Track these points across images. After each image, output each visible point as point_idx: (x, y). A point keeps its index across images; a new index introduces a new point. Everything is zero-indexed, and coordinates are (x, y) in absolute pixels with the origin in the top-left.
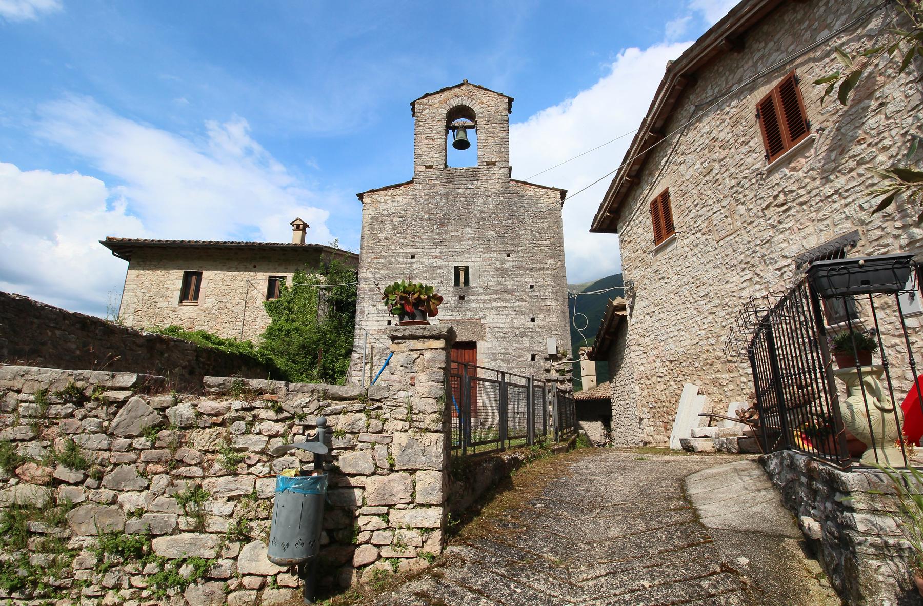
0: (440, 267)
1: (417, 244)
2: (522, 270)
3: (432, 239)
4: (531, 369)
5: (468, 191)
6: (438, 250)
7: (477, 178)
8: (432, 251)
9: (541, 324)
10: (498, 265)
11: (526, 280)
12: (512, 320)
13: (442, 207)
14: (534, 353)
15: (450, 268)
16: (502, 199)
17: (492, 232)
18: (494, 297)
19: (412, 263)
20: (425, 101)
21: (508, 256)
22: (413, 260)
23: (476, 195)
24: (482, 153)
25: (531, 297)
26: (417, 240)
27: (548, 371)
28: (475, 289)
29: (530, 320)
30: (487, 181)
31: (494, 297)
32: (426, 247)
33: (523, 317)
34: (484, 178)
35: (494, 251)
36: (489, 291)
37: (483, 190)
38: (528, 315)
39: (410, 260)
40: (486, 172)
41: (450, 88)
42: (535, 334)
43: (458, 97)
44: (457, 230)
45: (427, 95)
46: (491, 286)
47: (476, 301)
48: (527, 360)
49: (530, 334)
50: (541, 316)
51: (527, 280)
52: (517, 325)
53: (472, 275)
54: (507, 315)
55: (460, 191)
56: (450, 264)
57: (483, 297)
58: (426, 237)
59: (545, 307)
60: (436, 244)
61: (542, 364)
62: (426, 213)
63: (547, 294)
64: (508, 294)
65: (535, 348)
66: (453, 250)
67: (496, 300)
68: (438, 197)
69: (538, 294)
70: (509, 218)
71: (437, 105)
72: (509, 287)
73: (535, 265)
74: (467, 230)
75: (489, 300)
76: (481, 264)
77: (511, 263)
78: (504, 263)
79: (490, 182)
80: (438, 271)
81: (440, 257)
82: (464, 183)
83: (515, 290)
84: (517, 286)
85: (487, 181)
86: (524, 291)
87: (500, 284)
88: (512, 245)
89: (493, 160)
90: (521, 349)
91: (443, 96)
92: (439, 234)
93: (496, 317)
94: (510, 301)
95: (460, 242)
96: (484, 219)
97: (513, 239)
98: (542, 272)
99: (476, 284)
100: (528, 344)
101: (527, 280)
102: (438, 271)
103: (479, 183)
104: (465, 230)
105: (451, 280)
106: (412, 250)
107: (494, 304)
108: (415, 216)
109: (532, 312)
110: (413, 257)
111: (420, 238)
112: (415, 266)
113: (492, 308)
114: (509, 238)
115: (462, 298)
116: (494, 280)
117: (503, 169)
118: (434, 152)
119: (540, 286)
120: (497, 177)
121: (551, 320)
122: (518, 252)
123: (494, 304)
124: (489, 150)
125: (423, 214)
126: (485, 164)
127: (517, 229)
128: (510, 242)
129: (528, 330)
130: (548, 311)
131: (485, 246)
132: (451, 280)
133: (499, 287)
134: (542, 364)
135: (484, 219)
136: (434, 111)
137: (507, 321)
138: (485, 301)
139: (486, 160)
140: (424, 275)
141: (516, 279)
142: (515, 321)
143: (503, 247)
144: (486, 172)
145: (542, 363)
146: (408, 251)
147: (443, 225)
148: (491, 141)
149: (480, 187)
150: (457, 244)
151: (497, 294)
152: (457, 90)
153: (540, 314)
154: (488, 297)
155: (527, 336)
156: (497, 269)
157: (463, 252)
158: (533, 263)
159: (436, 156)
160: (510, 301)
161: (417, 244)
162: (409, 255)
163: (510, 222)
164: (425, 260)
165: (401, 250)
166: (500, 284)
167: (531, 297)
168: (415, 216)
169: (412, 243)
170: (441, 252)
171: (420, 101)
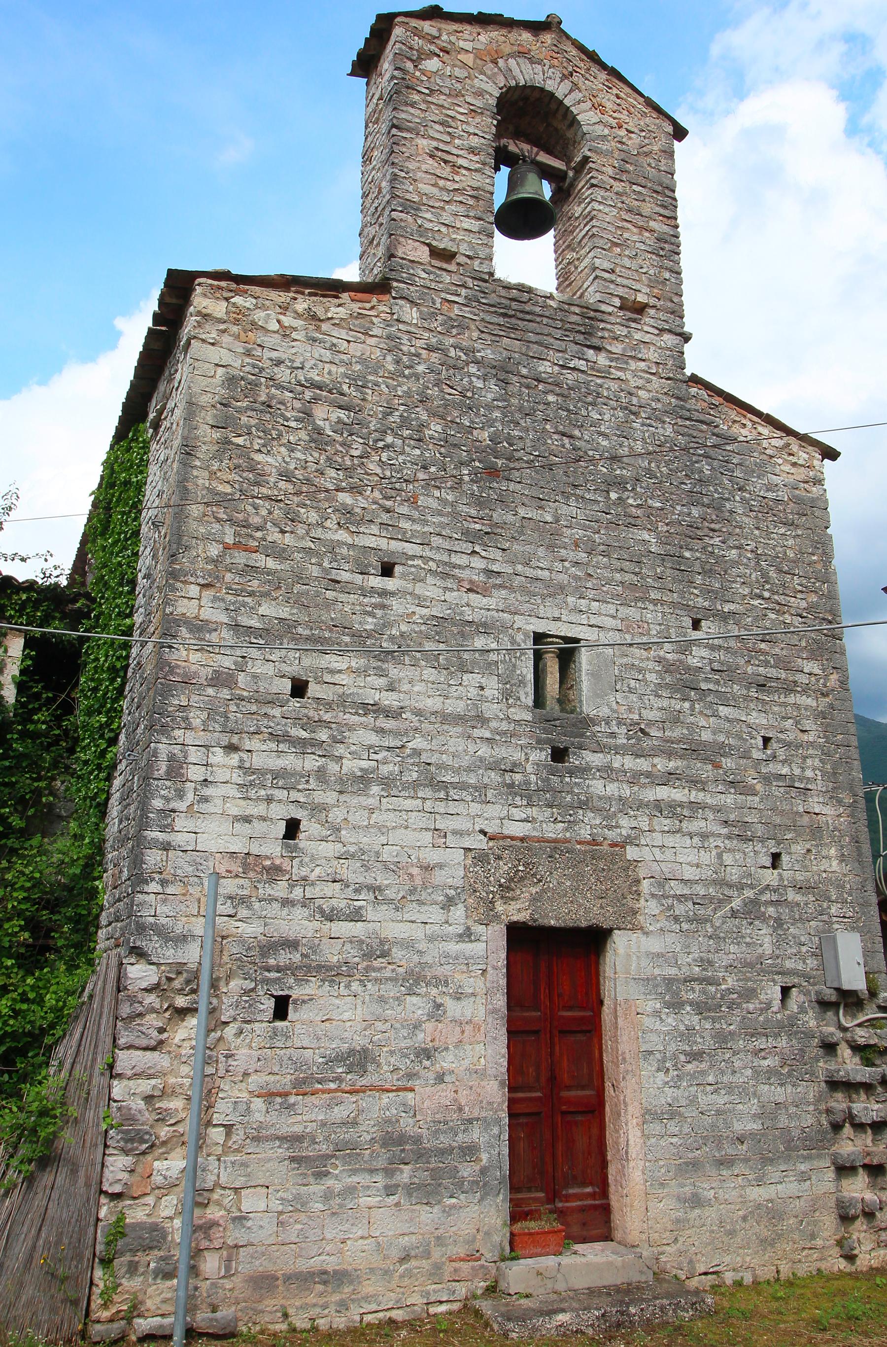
0: (484, 628)
1: (405, 525)
2: (739, 682)
3: (455, 515)
4: (783, 1043)
5: (570, 377)
6: (478, 563)
7: (595, 342)
8: (456, 559)
9: (799, 877)
10: (668, 652)
11: (751, 719)
12: (720, 856)
13: (489, 407)
14: (789, 981)
15: (519, 637)
16: (669, 431)
17: (646, 536)
18: (661, 764)
19: (384, 593)
20: (427, 26)
21: (696, 625)
22: (390, 584)
23: (595, 398)
24: (607, 265)
25: (767, 779)
26: (404, 509)
27: (829, 1048)
28: (603, 728)
29: (768, 862)
30: (624, 358)
31: (661, 764)
32: (436, 541)
33: (749, 848)
34: (617, 348)
35: (655, 602)
36: (647, 743)
37: (614, 386)
38: (762, 840)
39: (376, 582)
40: (621, 331)
41: (510, 24)
42: (785, 911)
43: (532, 61)
44: (540, 502)
45: (434, 13)
46: (651, 723)
47: (608, 773)
48: (769, 1005)
49: (771, 911)
50: (799, 849)
51: (756, 718)
52: (734, 874)
53: (595, 675)
54: (704, 836)
55: (545, 367)
56: (519, 621)
57: (629, 762)
58: (434, 504)
59: (806, 819)
60: (470, 537)
61: (812, 1023)
62: (433, 414)
63: (809, 773)
64: (706, 760)
65: (789, 964)
66: (530, 572)
67: (670, 778)
68: (473, 369)
69: (785, 771)
70: (693, 497)
71: (469, 59)
72: (706, 736)
73: (773, 672)
74: (570, 509)
75: (648, 775)
76: (616, 637)
77: (705, 653)
78: (685, 647)
79: (633, 365)
80: (479, 642)
81: (484, 591)
82: (557, 344)
83: (722, 750)
84: (728, 734)
85: (624, 358)
86: (746, 756)
87: (676, 719)
88: (707, 592)
89: (641, 298)
90: (751, 965)
91: (486, 37)
92: (480, 503)
93: (670, 840)
94: (711, 787)
95: (551, 547)
96: (620, 484)
97: (707, 572)
98: (791, 699)
99: (605, 712)
100: (768, 949)
101: (756, 718)
102: (479, 642)
103: (602, 360)
104: (564, 510)
105: (522, 683)
106: (383, 544)
107: (663, 793)
108: (395, 418)
109: (774, 832)
110: (387, 570)
111: (412, 501)
112: (397, 606)
113: (658, 806)
114: (697, 568)
115: (559, 755)
116: (658, 703)
117: (666, 337)
118: (461, 209)
119: (788, 745)
120: (652, 355)
121: (825, 864)
122: (724, 617)
123: (663, 793)
124: (627, 262)
125: (424, 416)
126: (617, 302)
127: (717, 541)
128: (699, 579)
129: (766, 897)
130: (816, 832)
131: (628, 577)
132: (522, 683)
133: (677, 732)
134: (812, 1023)
135: (620, 484)
136: (458, 72)
137: (706, 858)
138: (634, 779)
139: (621, 291)
140: (429, 646)
141: (723, 711)
142: (728, 859)
143: (682, 593)
144: (621, 331)
145: (810, 1020)
146: (371, 542)
147: (493, 472)
148: (632, 235)
149: (604, 373)
150: (541, 552)
151: (670, 755)
152: (526, 36)
153: (794, 841)
154: (643, 764)
155: (763, 918)
156: (668, 667)
157: (562, 588)
158: (766, 664)
159: (467, 224)
160: (711, 787)
161: (405, 525)
162: (374, 560)
163: (695, 512)
164: (431, 589)
165: (342, 536)
166: (676, 719)
167: (767, 779)
168: (395, 418)
169: (385, 517)
170: (489, 573)
171: (414, 23)
